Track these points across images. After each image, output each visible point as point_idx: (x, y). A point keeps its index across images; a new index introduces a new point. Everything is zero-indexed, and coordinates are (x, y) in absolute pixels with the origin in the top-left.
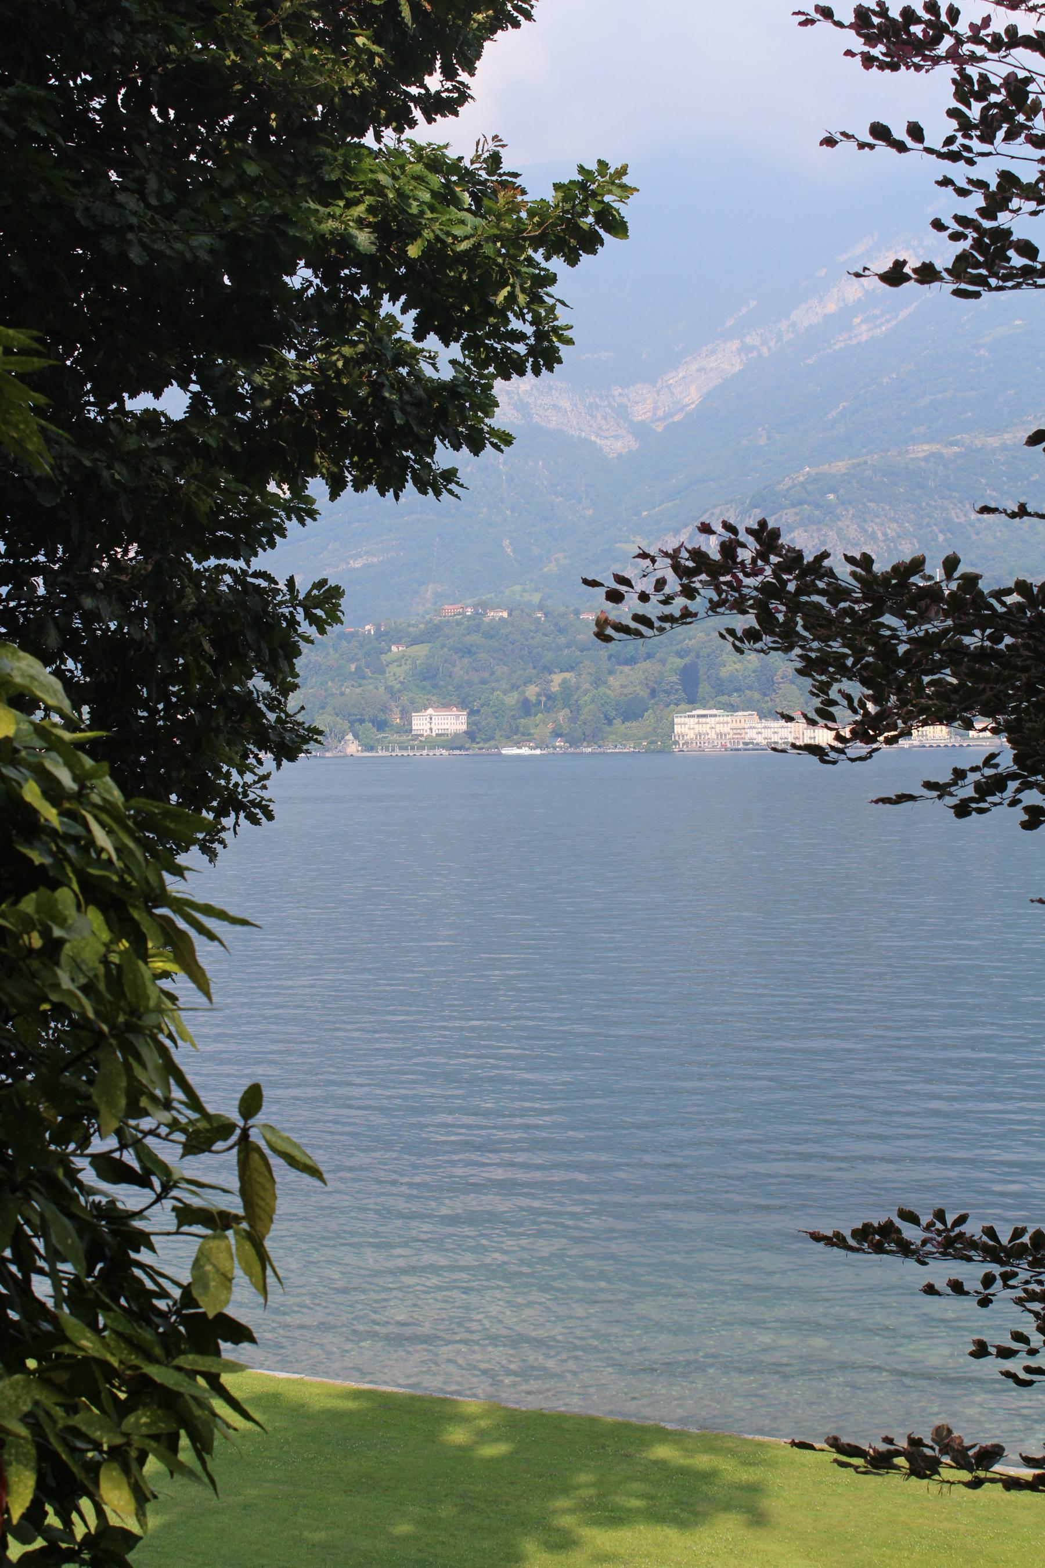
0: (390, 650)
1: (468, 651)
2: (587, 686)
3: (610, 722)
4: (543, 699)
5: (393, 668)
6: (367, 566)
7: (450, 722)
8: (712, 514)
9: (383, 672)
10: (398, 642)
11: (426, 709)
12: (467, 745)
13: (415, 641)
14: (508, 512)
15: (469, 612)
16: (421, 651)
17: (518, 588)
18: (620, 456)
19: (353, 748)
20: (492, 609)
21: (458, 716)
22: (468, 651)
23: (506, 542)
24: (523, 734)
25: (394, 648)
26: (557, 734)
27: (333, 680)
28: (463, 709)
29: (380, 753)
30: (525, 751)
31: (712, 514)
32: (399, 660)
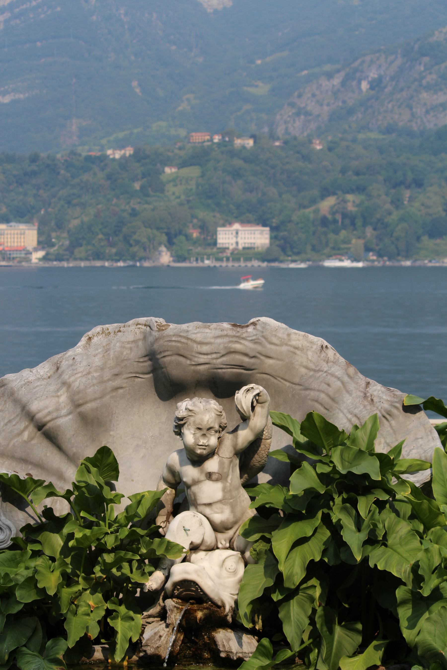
0: (164, 172)
1: (236, 174)
2: (388, 206)
3: (418, 239)
4: (339, 217)
5: (170, 189)
6: (13, 102)
7: (257, 237)
8: (363, 62)
9: (162, 191)
10: (171, 166)
11: (231, 224)
12: (282, 258)
13: (183, 165)
14: (133, 58)
15: (217, 139)
16: (193, 172)
17: (163, 124)
18: (216, 12)
19: (165, 258)
20: (239, 137)
21: (262, 231)
22: (236, 174)
23: (135, 84)
24: (333, 248)
25: (168, 170)
26: (368, 249)
27: (118, 198)
28: (265, 225)
29: (194, 264)
30: (347, 264)
31: (363, 62)
32: (174, 180)
